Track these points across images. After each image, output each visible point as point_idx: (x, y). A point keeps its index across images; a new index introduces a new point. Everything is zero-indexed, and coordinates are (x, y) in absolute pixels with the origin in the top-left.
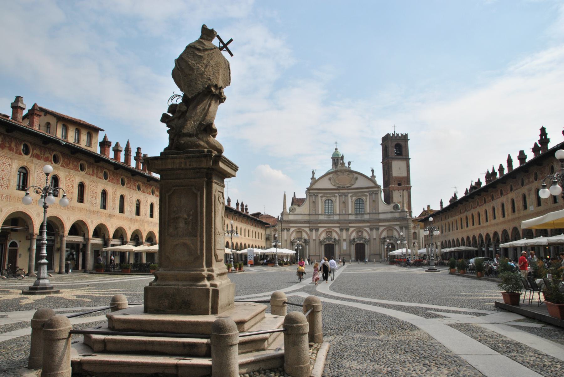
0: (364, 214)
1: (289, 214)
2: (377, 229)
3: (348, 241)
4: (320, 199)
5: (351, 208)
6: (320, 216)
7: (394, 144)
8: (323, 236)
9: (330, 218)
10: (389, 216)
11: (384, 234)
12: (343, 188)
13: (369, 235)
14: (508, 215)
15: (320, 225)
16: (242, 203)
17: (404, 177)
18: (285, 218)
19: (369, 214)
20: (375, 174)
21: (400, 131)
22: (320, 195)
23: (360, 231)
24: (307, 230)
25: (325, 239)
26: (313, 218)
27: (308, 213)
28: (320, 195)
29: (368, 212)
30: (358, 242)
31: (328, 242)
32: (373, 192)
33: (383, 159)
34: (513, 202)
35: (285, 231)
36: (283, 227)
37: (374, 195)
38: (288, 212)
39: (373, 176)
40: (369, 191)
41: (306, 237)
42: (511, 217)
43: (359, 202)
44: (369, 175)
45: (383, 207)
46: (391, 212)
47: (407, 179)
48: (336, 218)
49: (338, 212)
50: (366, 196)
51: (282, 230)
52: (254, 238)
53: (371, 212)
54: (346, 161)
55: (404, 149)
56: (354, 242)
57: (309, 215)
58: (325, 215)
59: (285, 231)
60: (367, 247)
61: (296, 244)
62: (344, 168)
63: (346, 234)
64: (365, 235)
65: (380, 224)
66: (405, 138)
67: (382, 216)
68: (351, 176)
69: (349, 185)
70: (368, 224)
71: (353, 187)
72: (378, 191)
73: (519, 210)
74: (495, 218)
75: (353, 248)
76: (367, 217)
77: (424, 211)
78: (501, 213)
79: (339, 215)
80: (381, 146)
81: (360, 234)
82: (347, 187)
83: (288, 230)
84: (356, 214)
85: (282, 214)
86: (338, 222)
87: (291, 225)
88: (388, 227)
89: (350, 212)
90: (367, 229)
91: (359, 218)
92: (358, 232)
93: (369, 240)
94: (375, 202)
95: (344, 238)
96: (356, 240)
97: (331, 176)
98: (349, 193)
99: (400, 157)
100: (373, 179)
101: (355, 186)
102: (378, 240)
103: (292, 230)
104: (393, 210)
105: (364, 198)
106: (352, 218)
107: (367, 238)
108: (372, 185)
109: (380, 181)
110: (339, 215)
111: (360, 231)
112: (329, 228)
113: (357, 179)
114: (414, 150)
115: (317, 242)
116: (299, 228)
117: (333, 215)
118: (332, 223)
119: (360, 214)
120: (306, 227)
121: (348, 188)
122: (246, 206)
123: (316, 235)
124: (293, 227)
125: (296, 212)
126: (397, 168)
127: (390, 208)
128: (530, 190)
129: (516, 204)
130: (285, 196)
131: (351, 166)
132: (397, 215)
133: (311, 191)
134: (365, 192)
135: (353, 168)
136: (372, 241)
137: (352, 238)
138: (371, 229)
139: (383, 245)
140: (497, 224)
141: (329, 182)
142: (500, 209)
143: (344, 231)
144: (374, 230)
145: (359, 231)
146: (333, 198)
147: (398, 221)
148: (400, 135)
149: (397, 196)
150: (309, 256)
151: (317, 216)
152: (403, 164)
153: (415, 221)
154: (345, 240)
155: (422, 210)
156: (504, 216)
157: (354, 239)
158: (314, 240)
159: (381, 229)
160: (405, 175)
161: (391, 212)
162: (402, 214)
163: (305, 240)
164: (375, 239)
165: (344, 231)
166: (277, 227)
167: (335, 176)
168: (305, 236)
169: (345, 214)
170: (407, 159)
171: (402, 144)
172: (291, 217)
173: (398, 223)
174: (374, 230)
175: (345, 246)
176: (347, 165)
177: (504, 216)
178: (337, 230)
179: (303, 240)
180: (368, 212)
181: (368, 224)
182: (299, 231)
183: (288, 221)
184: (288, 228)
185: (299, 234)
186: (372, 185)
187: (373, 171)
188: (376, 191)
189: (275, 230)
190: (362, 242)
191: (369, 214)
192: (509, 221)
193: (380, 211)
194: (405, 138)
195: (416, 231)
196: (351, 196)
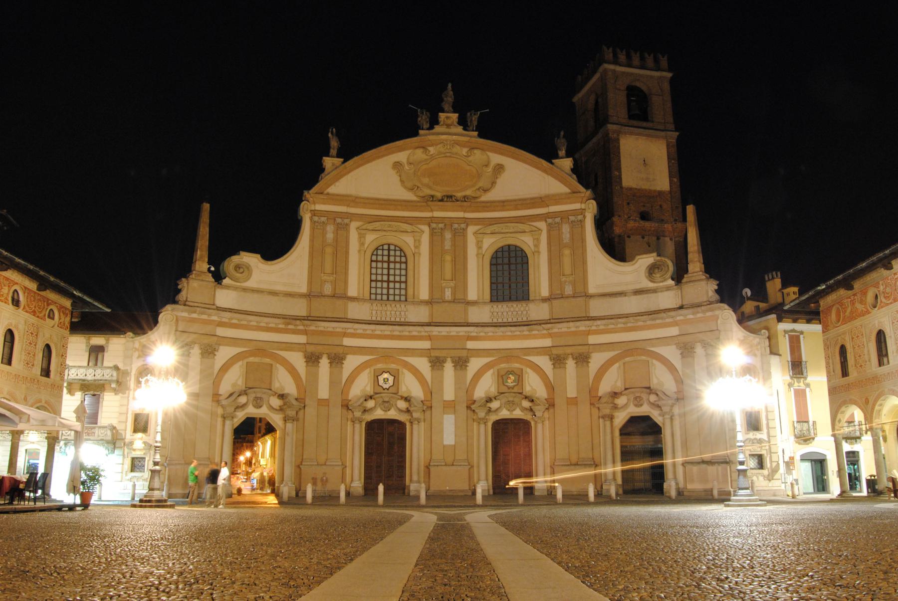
5: (477, 281)
8: (362, 386)
13: (550, 387)
17: (660, 193)
26: (323, 307)
27: (304, 289)
29: (545, 292)
31: (379, 414)
41: (289, 387)
46: (638, 292)
49: (424, 294)
57: (309, 296)
63: (458, 382)
64: (534, 384)
72: (582, 212)
75: (483, 438)
90: (544, 362)
92: (502, 377)
98: (467, 222)
99: (645, 124)
101: (495, 194)
104: (647, 284)
105: (526, 242)
111: (512, 372)
120: (289, 347)
123: (333, 383)
124: (234, 342)
125: (251, 283)
141: (394, 178)
143: (449, 367)
146: (409, 240)
151: (339, 302)
154: (450, 406)
161: (638, 292)
164: (573, 402)
165: (449, 367)
168: (284, 382)
169: (454, 301)
175: (449, 430)
178: (423, 364)
188: (574, 212)
196: (475, 233)
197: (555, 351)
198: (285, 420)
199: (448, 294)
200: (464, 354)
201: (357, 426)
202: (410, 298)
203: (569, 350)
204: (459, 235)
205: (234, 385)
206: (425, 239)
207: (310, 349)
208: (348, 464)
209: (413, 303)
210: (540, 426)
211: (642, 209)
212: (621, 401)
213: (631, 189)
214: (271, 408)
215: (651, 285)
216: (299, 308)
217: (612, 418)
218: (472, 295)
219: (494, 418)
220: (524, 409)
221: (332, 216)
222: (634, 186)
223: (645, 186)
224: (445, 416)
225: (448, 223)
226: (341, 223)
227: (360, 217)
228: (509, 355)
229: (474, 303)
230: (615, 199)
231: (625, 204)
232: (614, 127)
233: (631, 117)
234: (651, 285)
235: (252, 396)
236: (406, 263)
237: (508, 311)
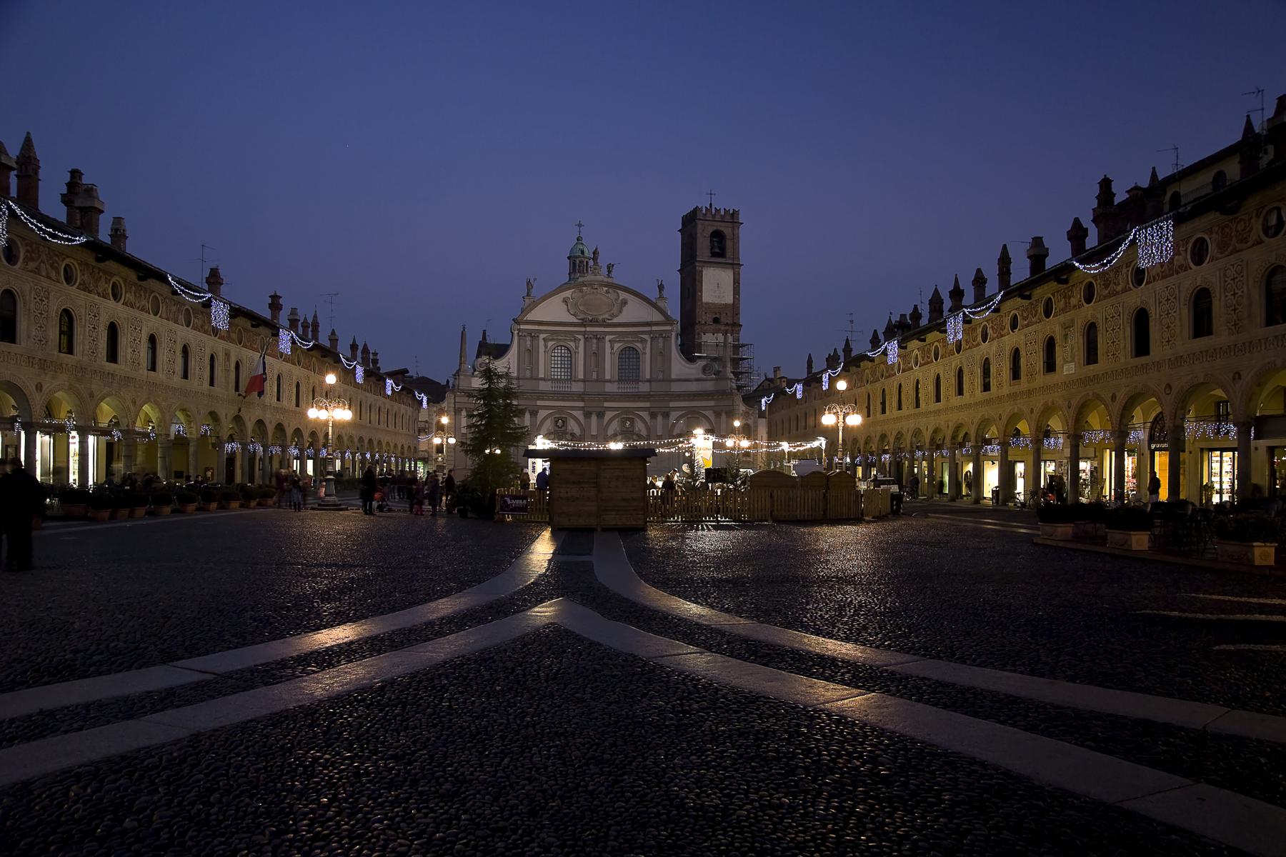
0: (637, 381)
5: (610, 369)
7: (711, 230)
9: (563, 388)
10: (693, 387)
12: (594, 322)
13: (648, 429)
14: (1000, 385)
15: (539, 403)
16: (365, 346)
20: (665, 293)
21: (723, 203)
22: (542, 336)
23: (628, 419)
29: (648, 377)
32: (660, 333)
34: (1016, 355)
37: (661, 340)
39: (661, 297)
40: (651, 332)
42: (1006, 390)
43: (629, 358)
44: (653, 294)
45: (679, 366)
46: (697, 380)
47: (735, 308)
48: (577, 388)
49: (581, 376)
50: (643, 341)
52: (391, 427)
54: (603, 262)
55: (729, 244)
62: (599, 278)
66: (733, 218)
67: (676, 388)
68: (612, 296)
69: (606, 316)
70: (648, 405)
71: (615, 320)
73: (1031, 375)
74: (960, 392)
76: (644, 388)
78: (978, 381)
79: (584, 381)
84: (620, 381)
85: (457, 374)
86: (580, 396)
89: (608, 377)
90: (645, 414)
91: (629, 388)
92: (623, 422)
94: (664, 355)
95: (594, 432)
97: (568, 294)
100: (660, 304)
106: (610, 388)
108: (657, 317)
109: (674, 311)
110: (584, 381)
111: (628, 419)
112: (560, 409)
113: (624, 303)
114: (748, 241)
117: (572, 379)
119: (628, 381)
122: (375, 354)
127: (694, 370)
128: (1067, 327)
129: (1023, 361)
131: (612, 274)
132: (709, 386)
134: (643, 333)
135: (617, 278)
138: (653, 416)
140: (968, 406)
142: (979, 371)
143: (594, 418)
144: (660, 418)
146: (572, 344)
152: (726, 276)
156: (986, 387)
160: (729, 300)
161: (697, 380)
165: (594, 418)
166: (444, 405)
167: (578, 294)
169: (597, 381)
170: (735, 265)
171: (727, 230)
173: (712, 403)
174: (660, 418)
177: (986, 387)
178: (579, 414)
180: (648, 377)
181: (648, 405)
186: (657, 317)
187: (661, 287)
192: (1000, 399)
193: (673, 377)
194: (733, 218)
195: (750, 422)
199: (594, 376)
204: (600, 338)
218: (608, 377)
221: (530, 333)
223: (717, 301)
225: (595, 335)
226: (534, 336)
227: (545, 331)
228: (626, 410)
233: (714, 255)
237: (629, 388)
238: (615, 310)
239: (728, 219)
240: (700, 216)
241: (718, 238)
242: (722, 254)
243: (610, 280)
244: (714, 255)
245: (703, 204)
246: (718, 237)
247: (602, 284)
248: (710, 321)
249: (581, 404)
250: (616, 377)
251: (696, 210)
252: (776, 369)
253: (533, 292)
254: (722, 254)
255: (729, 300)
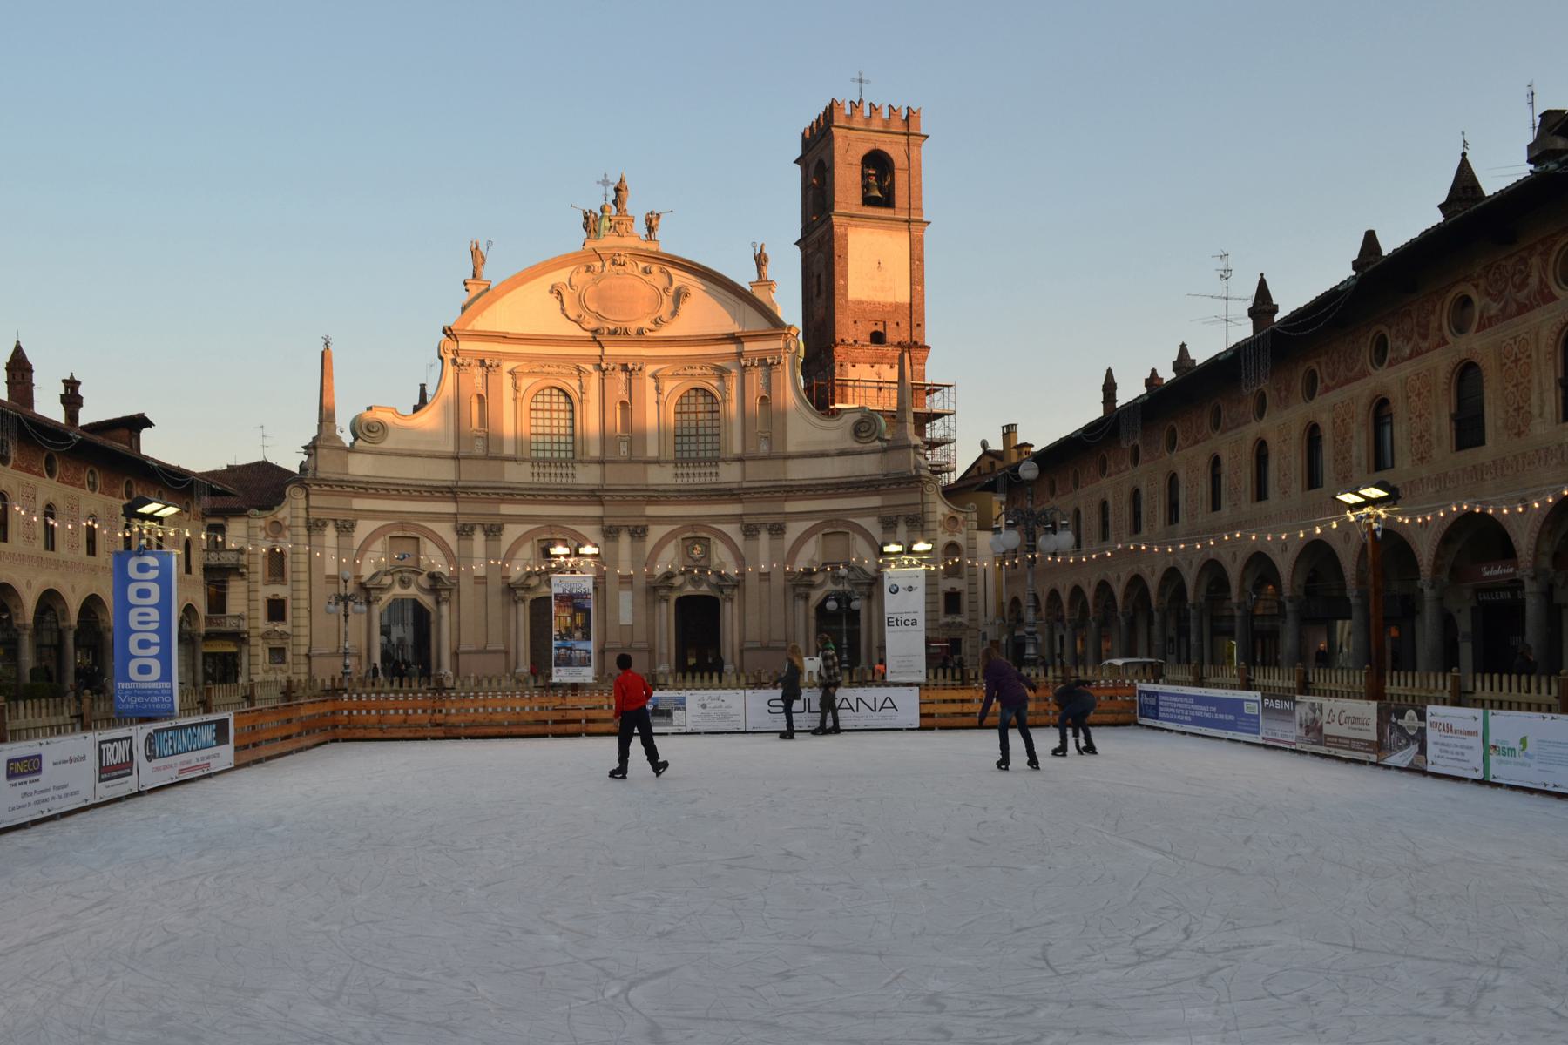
0: (715, 461)
1: (351, 449)
2: (777, 530)
3: (641, 583)
4: (507, 381)
6: (509, 466)
7: (864, 149)
9: (555, 478)
11: (808, 556)
13: (740, 560)
15: (506, 509)
17: (897, 307)
18: (328, 467)
19: (740, 459)
21: (886, 94)
24: (445, 531)
25: (529, 575)
26: (475, 474)
27: (450, 448)
28: (507, 366)
30: (689, 590)
33: (804, 230)
35: (330, 532)
36: (314, 514)
38: (347, 438)
41: (441, 566)
44: (744, 276)
45: (805, 431)
46: (842, 453)
47: (914, 312)
51: (314, 526)
53: (751, 450)
54: (637, 207)
55: (900, 179)
56: (671, 588)
57: (456, 458)
58: (533, 461)
59: (330, 532)
60: (730, 615)
61: (386, 598)
62: (629, 242)
65: (791, 507)
66: (909, 125)
67: (799, 472)
69: (646, 324)
75: (666, 615)
76: (729, 474)
77: (987, 453)
79: (601, 462)
80: (797, 171)
81: (697, 551)
82: (640, 332)
83: (345, 528)
84: (677, 462)
85: (311, 449)
86: (594, 496)
87: (359, 504)
88: (829, 523)
90: (732, 530)
91: (697, 478)
93: (738, 583)
95: (625, 568)
96: (678, 581)
97: (561, 277)
100: (760, 294)
102: (778, 582)
103: (364, 528)
106: (661, 477)
107: (732, 570)
109: (789, 306)
110: (601, 462)
111: (697, 540)
115: (496, 584)
116: (403, 520)
118: (567, 503)
119: (697, 462)
120: (438, 517)
121: (640, 338)
126: (872, 262)
127: (833, 434)
130: (325, 358)
131: (658, 234)
132: (867, 466)
133: (464, 345)
135: (669, 242)
136: (752, 583)
137: (659, 570)
138: (750, 531)
139: (801, 603)
143: (625, 540)
144: (764, 537)
145: (696, 537)
147: (877, 492)
148: (886, 115)
149: (867, 382)
150: (456, 654)
153: (950, 492)
154: (627, 580)
155: (980, 451)
157: (669, 576)
158: (481, 580)
159: (795, 530)
160: (903, 296)
161: (842, 453)
162: (896, 457)
163: (433, 577)
164: (765, 576)
167: (582, 278)
169: (630, 461)
170: (913, 223)
171: (896, 152)
172: (360, 467)
174: (764, 537)
175: (625, 609)
176: (640, 228)
179: (423, 580)
180: (737, 449)
181: (735, 509)
182: (406, 535)
183: (341, 483)
184: (340, 516)
185: (408, 547)
186: (761, 325)
187: (761, 260)
189: (277, 528)
190: (704, 589)
191: (740, 459)
193: (792, 448)
195: (960, 539)
197: (747, 520)
198: (438, 603)
200: (643, 522)
201: (521, 606)
202: (578, 457)
203: (763, 519)
205: (377, 564)
206: (594, 381)
207: (462, 519)
208: (512, 650)
209: (582, 462)
210: (728, 605)
211: (875, 328)
212: (818, 579)
213: (859, 302)
214: (420, 588)
215: (856, 446)
216: (444, 473)
217: (807, 598)
219: (674, 596)
220: (710, 585)
222: (864, 298)
224: (622, 593)
228: (694, 523)
229: (657, 462)
230: (838, 317)
231: (851, 323)
232: (843, 220)
233: (868, 201)
234: (856, 446)
235: (397, 577)
236: (572, 411)
238: (665, 312)
239: (897, 126)
240: (839, 120)
241: (877, 164)
242: (886, 200)
243: (652, 247)
244: (868, 201)
245: (846, 94)
246: (877, 164)
247: (639, 255)
248: (865, 338)
249: (595, 511)
250: (670, 455)
251: (829, 114)
252: (1009, 431)
253: (487, 273)
254: (887, 201)
255: (903, 296)
